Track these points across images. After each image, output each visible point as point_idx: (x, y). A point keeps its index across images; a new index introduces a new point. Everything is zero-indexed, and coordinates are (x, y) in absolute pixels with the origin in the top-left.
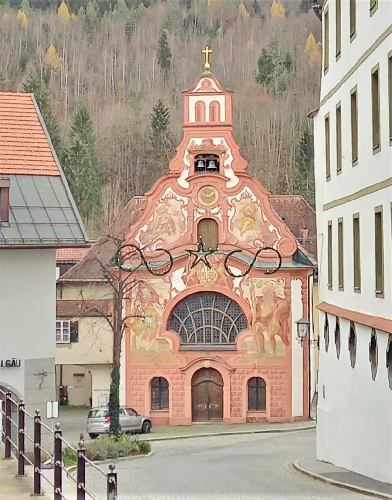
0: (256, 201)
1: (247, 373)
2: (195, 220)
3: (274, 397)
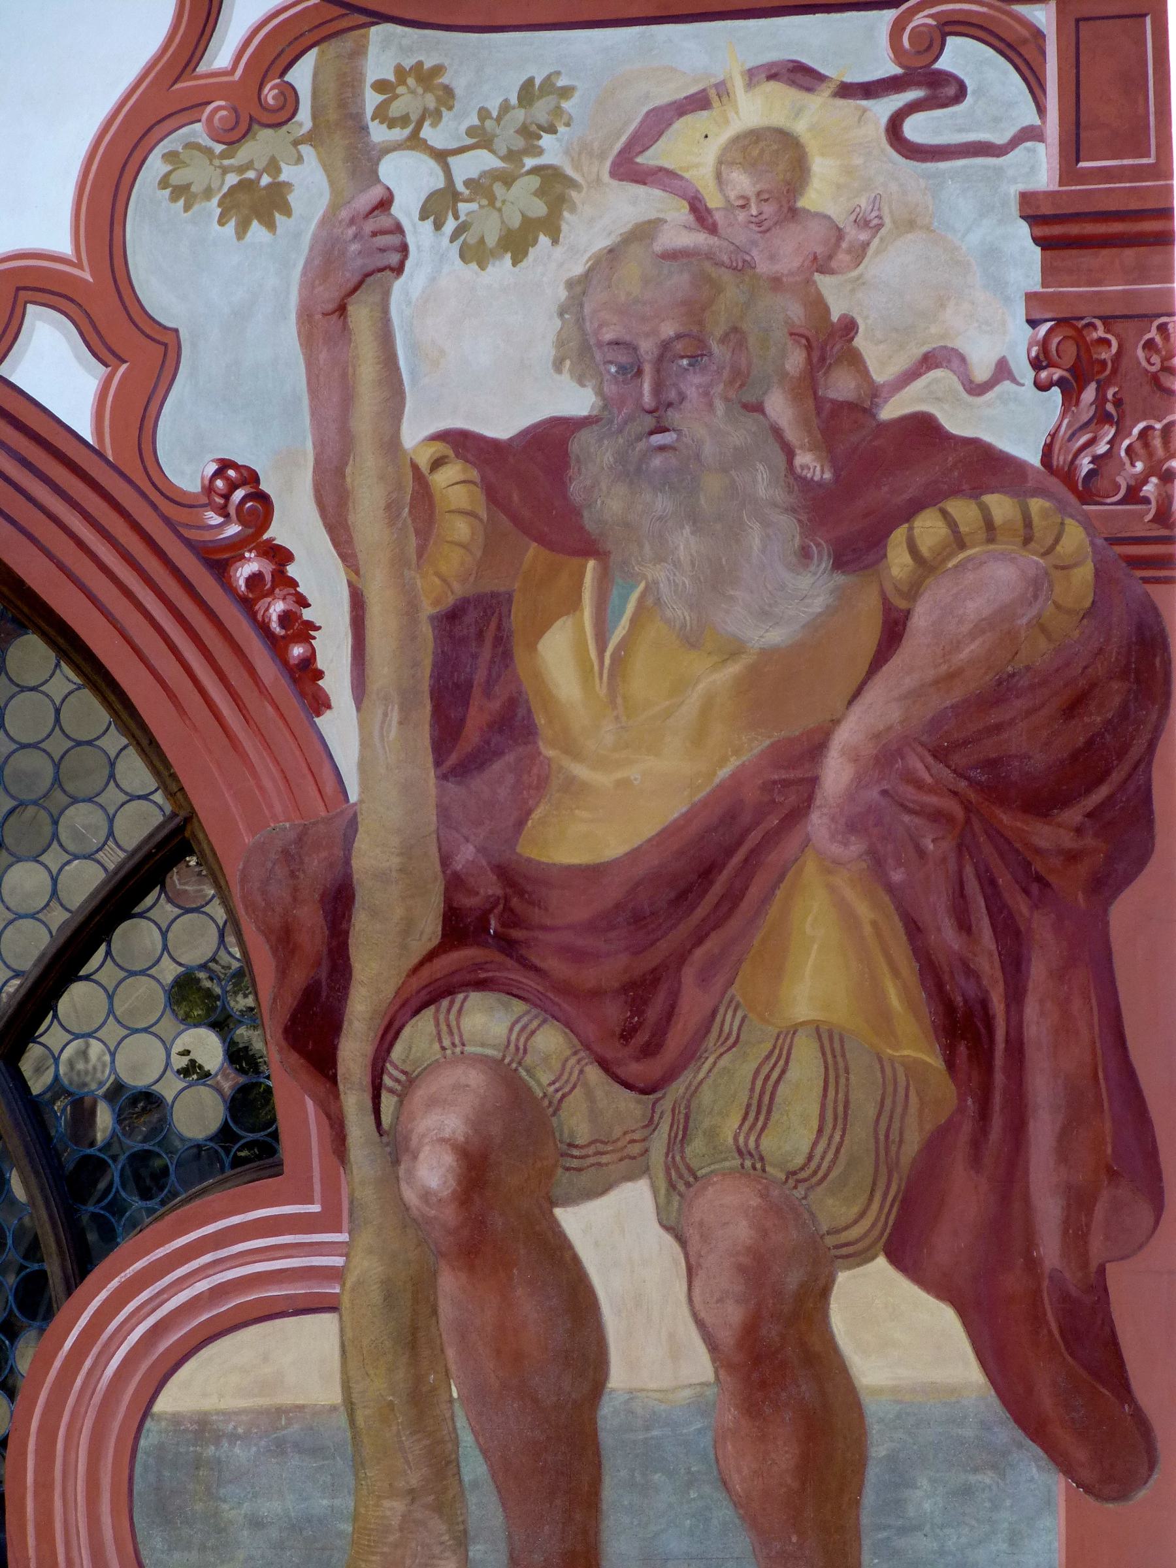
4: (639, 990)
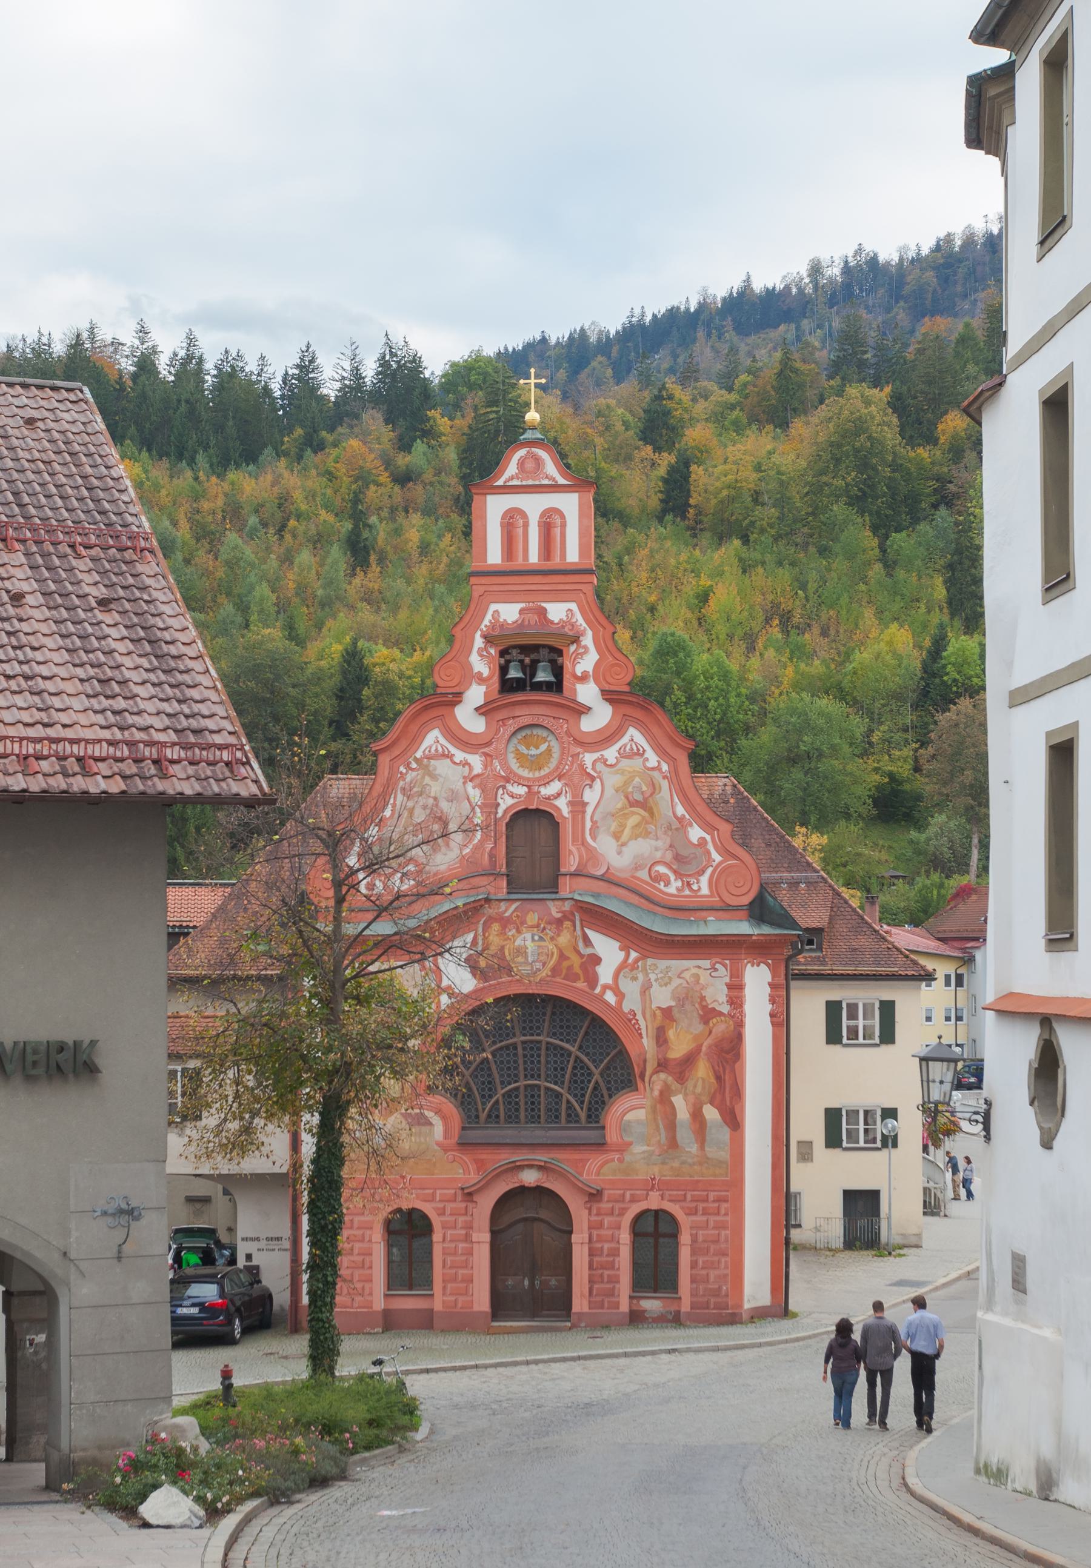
0: (656, 764)
2: (500, 815)
4: (681, 1073)
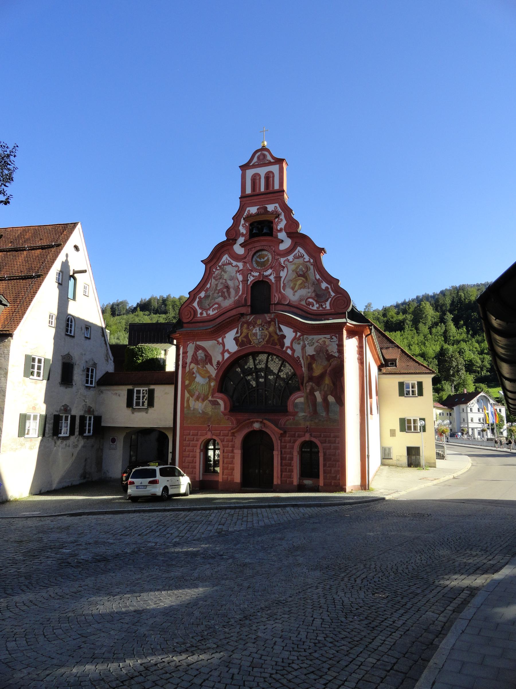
1: (298, 437)
3: (328, 463)
